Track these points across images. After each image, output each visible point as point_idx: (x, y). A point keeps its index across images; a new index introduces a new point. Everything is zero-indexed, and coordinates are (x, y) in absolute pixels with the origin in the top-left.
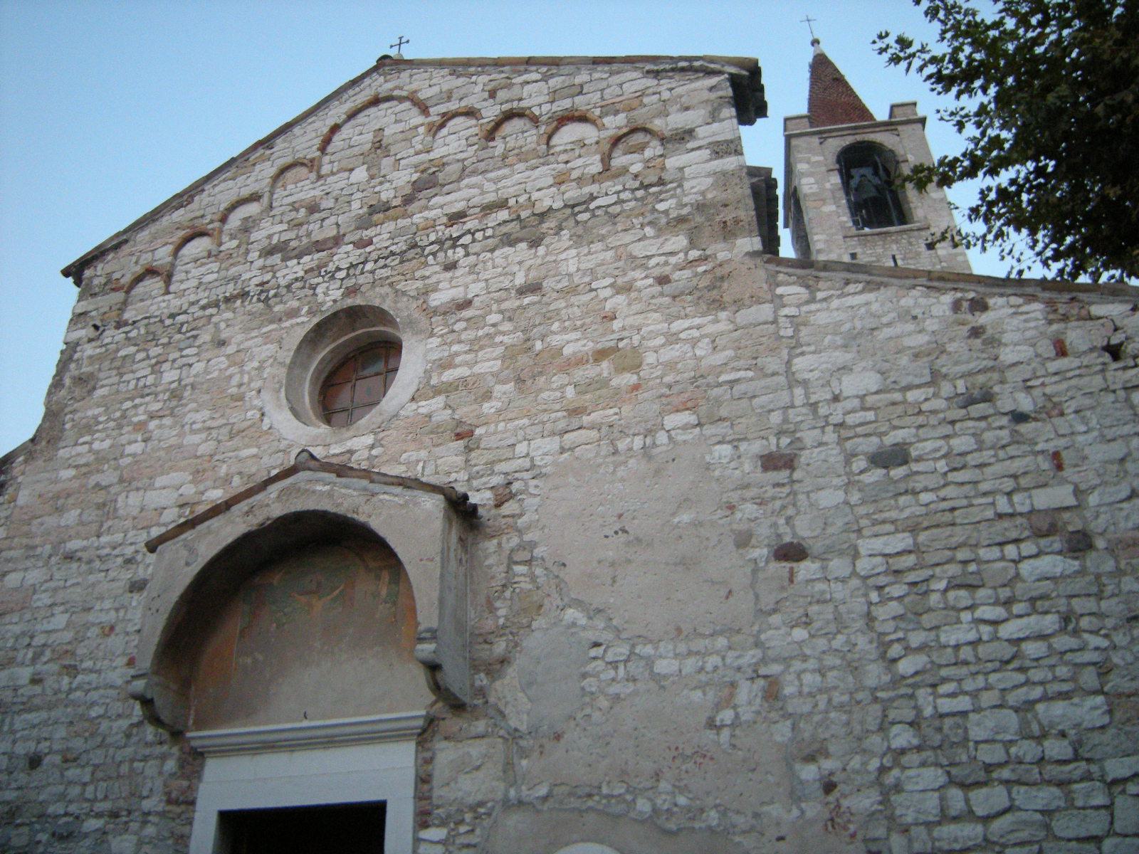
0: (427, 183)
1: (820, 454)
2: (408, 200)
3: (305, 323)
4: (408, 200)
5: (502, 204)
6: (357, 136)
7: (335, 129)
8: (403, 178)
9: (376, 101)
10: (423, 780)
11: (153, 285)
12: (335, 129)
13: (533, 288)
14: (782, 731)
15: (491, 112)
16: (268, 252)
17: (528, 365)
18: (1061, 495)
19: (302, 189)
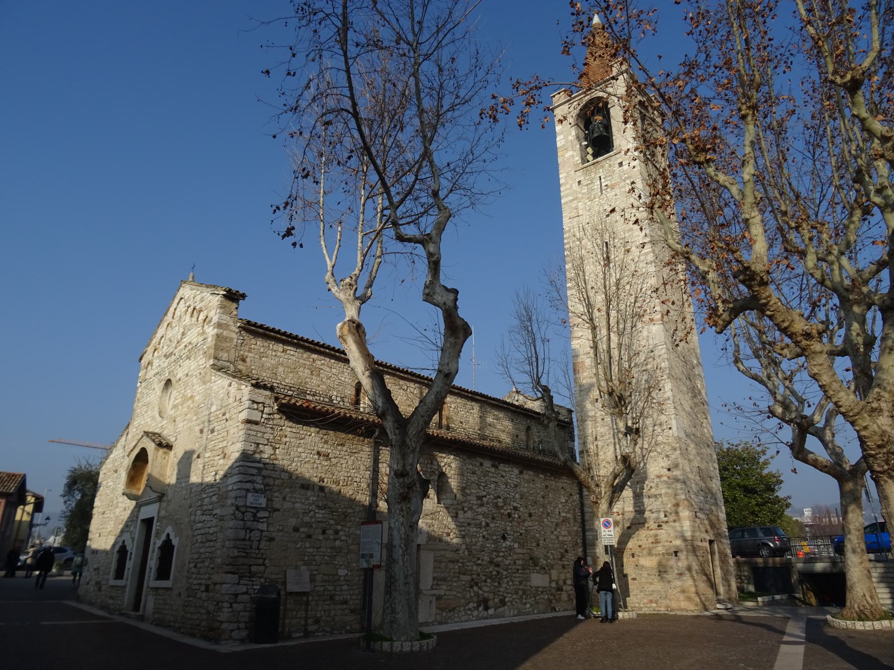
0: (183, 334)
1: (205, 430)
2: (181, 339)
3: (163, 382)
4: (181, 339)
5: (190, 343)
6: (178, 313)
7: (175, 309)
8: (181, 330)
9: (181, 299)
10: (159, 512)
11: (150, 367)
12: (175, 309)
13: (187, 375)
14: (189, 502)
15: (192, 307)
16: (165, 356)
17: (185, 399)
18: (225, 444)
19: (170, 334)
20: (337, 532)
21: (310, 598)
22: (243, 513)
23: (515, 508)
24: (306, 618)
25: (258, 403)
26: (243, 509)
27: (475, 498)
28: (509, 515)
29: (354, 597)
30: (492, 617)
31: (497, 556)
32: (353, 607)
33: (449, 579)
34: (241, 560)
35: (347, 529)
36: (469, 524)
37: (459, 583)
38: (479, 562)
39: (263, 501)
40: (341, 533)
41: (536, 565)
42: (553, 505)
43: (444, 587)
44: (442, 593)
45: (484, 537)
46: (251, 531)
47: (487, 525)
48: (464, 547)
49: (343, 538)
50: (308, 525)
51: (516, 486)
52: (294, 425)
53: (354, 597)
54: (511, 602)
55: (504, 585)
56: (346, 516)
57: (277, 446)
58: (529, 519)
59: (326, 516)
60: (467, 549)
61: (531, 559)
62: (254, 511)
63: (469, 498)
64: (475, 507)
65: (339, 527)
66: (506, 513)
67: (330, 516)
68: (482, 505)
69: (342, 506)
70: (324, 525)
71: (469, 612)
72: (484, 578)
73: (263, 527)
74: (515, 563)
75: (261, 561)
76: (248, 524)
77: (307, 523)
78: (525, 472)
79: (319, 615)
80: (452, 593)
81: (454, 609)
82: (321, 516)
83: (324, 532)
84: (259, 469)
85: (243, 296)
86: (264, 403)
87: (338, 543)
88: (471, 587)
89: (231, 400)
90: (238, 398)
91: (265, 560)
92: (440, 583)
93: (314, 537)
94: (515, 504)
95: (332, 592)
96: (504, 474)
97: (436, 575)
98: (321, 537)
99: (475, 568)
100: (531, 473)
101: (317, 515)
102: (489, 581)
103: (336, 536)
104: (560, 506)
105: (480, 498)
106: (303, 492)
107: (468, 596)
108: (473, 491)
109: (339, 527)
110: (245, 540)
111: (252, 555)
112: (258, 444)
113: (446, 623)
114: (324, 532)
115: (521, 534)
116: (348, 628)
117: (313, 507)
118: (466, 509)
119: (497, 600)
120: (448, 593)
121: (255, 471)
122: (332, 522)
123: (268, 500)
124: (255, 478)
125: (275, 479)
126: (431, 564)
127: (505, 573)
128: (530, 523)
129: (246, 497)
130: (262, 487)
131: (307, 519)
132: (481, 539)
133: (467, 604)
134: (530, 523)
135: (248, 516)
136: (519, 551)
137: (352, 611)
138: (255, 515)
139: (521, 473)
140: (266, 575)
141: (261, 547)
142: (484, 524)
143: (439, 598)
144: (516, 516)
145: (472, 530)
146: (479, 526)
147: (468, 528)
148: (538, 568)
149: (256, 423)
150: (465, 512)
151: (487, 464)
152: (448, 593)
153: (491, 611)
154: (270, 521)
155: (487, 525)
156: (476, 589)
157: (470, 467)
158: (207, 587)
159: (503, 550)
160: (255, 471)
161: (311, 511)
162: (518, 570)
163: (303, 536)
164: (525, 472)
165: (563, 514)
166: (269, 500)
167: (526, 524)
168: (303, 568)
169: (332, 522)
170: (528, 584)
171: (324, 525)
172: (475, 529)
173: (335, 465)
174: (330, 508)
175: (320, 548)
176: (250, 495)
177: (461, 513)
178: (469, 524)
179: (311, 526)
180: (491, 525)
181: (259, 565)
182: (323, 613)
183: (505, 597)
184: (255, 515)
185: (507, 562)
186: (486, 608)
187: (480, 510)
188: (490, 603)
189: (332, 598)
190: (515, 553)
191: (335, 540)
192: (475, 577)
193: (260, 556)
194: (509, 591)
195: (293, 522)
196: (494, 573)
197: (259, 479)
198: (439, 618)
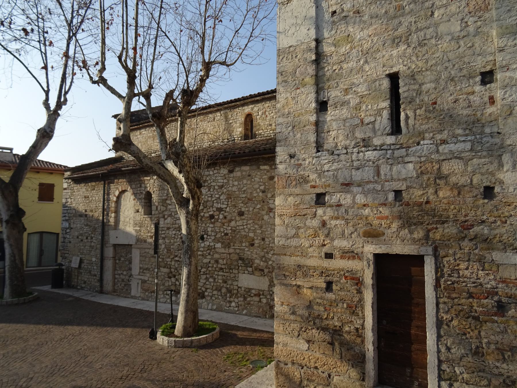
20: (92, 238)
23: (220, 210)
28: (212, 217)
33: (151, 269)
36: (168, 228)
38: (177, 259)
40: (94, 238)
44: (146, 279)
49: (94, 241)
50: (81, 235)
51: (221, 187)
60: (165, 247)
61: (240, 259)
65: (93, 235)
66: (207, 215)
83: (87, 238)
87: (93, 244)
88: (170, 278)
92: (145, 271)
97: (141, 266)
103: (91, 240)
113: (148, 300)
114: (87, 238)
115: (226, 234)
117: (83, 226)
118: (166, 217)
122: (90, 233)
125: (71, 214)
131: (81, 232)
136: (223, 250)
143: (144, 282)
144: (221, 216)
145: (170, 233)
147: (167, 232)
150: (165, 219)
162: (221, 269)
163: (80, 240)
166: (70, 224)
167: (233, 224)
170: (235, 283)
171: (86, 234)
172: (174, 232)
178: (168, 228)
189: (90, 272)
190: (217, 253)
191: (91, 242)
195: (76, 234)
198: (142, 295)
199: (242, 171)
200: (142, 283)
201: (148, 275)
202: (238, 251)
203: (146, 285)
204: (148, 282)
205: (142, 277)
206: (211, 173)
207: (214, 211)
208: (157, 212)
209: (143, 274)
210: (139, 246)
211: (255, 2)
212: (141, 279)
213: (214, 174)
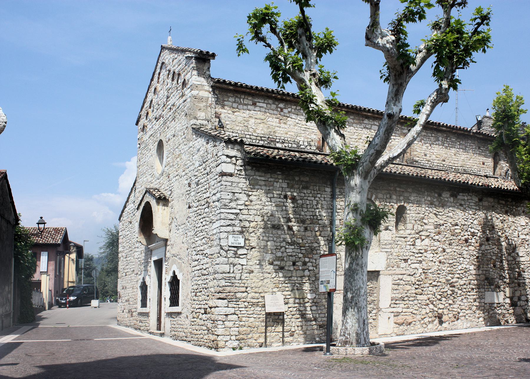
20: (305, 264)
21: (285, 317)
22: (226, 251)
24: (283, 331)
25: (231, 157)
26: (227, 248)
27: (432, 227)
28: (466, 241)
29: (322, 315)
30: (446, 329)
31: (452, 278)
32: (321, 323)
34: (228, 289)
35: (314, 261)
36: (426, 251)
37: (416, 302)
39: (241, 241)
40: (309, 264)
41: (491, 284)
42: (512, 228)
43: (402, 305)
45: (440, 262)
46: (234, 266)
47: (444, 250)
48: (421, 271)
49: (311, 268)
50: (281, 259)
52: (263, 174)
53: (322, 315)
54: (465, 316)
55: (458, 302)
56: (312, 250)
57: (250, 193)
58: (486, 243)
59: (296, 250)
61: (487, 279)
62: (235, 249)
63: (426, 227)
64: (432, 235)
65: (307, 260)
66: (463, 238)
67: (299, 251)
68: (439, 233)
69: (309, 242)
70: (294, 258)
71: (425, 326)
72: (439, 297)
73: (243, 261)
74: (470, 284)
75: (244, 289)
76: (231, 260)
77: (279, 257)
78: (485, 199)
79: (293, 330)
80: (408, 310)
81: (410, 324)
82: (291, 251)
83: (294, 264)
84: (237, 214)
85: (213, 56)
86: (236, 157)
88: (427, 305)
89: (210, 156)
90: (215, 154)
91: (247, 288)
92: (397, 302)
93: (286, 268)
94: (472, 230)
95: (304, 312)
96: (463, 203)
97: (394, 295)
98: (292, 268)
99: (430, 288)
100: (491, 200)
101: (288, 251)
102: (444, 299)
104: (520, 229)
105: (438, 226)
106: (274, 232)
107: (424, 312)
108: (430, 221)
109: (307, 260)
110: (229, 273)
111: (236, 284)
112: (234, 193)
116: (317, 339)
119: (450, 315)
120: (404, 310)
121: (233, 217)
122: (301, 255)
123: (245, 239)
124: (233, 222)
125: (250, 222)
126: (390, 286)
127: (460, 292)
128: (488, 247)
129: (227, 238)
130: (240, 229)
131: (279, 254)
132: (437, 263)
133: (423, 319)
134: (488, 247)
135: (230, 254)
137: (320, 326)
138: (236, 253)
139: (480, 200)
140: (248, 300)
141: (243, 278)
142: (440, 249)
143: (397, 315)
146: (435, 252)
147: (425, 254)
148: (492, 287)
149: (231, 175)
151: (446, 195)
152: (404, 310)
153: (444, 325)
154: (248, 257)
155: (444, 250)
156: (431, 306)
157: (429, 199)
158: (205, 309)
159: (459, 272)
160: (233, 217)
161: (281, 247)
162: (473, 289)
164: (485, 199)
165: (524, 237)
168: (279, 293)
169: (301, 255)
171: (294, 258)
172: (432, 255)
173: (302, 206)
174: (299, 244)
175: (291, 277)
176: (230, 236)
177: (418, 242)
179: (283, 260)
180: (448, 251)
181: (243, 292)
182: (296, 328)
183: (459, 313)
184: (236, 253)
185: (462, 282)
186: (441, 323)
187: (437, 237)
188: (444, 318)
191: (304, 270)
192: (430, 296)
193: (243, 285)
194: (463, 307)
196: (449, 292)
197: (237, 222)
198: (396, 330)
199: (489, 202)
200: (395, 316)
201: (402, 305)
202: (484, 272)
203: (400, 317)
204: (402, 314)
205: (394, 310)
206: (466, 198)
207: (469, 235)
208: (414, 231)
209: (395, 306)
210: (390, 272)
211: (392, 7)
212: (393, 312)
213: (468, 200)
